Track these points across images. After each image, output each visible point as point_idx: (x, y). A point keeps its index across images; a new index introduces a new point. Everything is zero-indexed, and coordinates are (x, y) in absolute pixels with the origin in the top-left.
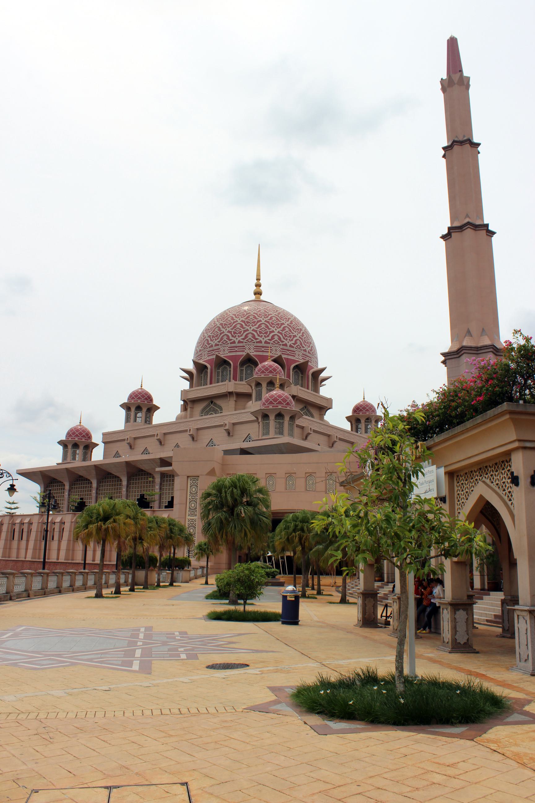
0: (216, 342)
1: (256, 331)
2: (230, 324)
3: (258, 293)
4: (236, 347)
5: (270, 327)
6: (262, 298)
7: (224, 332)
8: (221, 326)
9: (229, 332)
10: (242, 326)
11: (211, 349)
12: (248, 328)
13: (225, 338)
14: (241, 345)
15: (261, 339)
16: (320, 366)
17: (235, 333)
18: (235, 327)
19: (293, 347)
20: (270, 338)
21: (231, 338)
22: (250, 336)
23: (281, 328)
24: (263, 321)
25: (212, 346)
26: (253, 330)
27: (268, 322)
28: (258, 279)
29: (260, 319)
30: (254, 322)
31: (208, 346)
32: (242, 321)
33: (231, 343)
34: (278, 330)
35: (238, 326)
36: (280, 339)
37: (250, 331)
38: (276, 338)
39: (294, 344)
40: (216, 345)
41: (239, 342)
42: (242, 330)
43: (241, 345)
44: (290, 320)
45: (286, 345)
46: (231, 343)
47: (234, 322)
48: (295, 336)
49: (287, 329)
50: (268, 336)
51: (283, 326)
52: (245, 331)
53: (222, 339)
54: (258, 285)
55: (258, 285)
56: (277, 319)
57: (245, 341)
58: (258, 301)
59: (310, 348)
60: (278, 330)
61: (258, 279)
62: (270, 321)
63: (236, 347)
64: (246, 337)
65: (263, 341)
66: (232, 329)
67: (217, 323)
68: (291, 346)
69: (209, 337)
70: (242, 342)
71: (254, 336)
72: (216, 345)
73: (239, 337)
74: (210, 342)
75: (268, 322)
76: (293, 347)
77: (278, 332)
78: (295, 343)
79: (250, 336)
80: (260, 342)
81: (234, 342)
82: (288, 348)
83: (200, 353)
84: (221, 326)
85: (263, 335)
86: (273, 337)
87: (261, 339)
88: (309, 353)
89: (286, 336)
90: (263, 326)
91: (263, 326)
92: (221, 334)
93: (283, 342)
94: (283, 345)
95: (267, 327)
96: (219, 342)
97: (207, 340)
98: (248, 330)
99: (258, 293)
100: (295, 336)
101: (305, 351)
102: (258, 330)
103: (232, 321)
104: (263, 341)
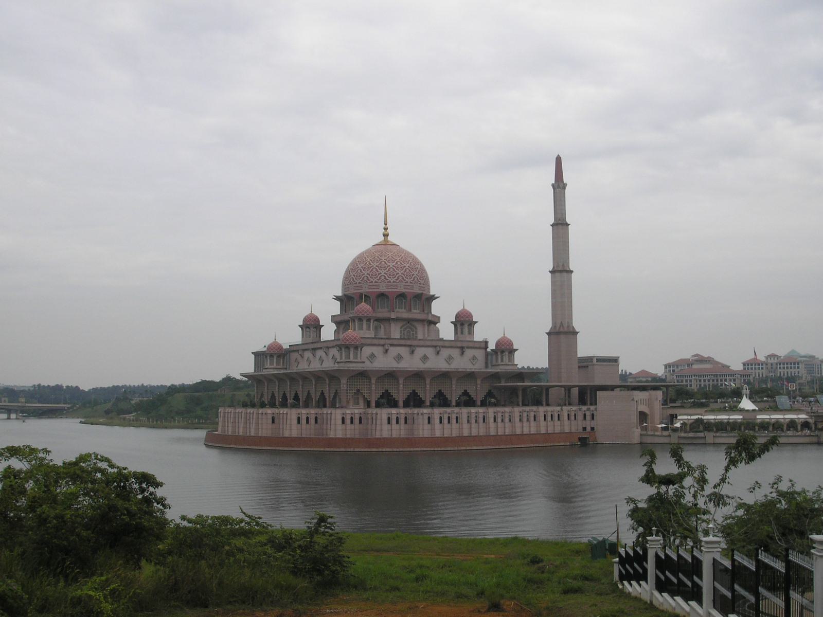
0: (359, 281)
1: (387, 274)
2: (368, 268)
3: (386, 235)
4: (374, 285)
5: (396, 270)
6: (389, 238)
7: (364, 274)
8: (362, 269)
9: (368, 274)
10: (377, 270)
11: (356, 285)
12: (381, 271)
13: (365, 278)
14: (377, 284)
15: (390, 279)
16: (432, 293)
17: (372, 275)
18: (372, 270)
19: (412, 283)
20: (396, 278)
21: (370, 279)
22: (383, 278)
23: (404, 271)
24: (391, 266)
25: (356, 283)
26: (385, 273)
27: (395, 267)
28: (386, 224)
29: (389, 264)
30: (385, 267)
31: (354, 283)
32: (377, 266)
33: (370, 283)
34: (401, 272)
35: (374, 270)
36: (403, 278)
37: (383, 274)
38: (401, 278)
39: (413, 281)
40: (359, 283)
41: (376, 282)
42: (377, 273)
43: (377, 284)
44: (410, 262)
45: (407, 282)
46: (370, 283)
47: (372, 267)
48: (413, 275)
49: (408, 271)
50: (395, 277)
51: (405, 268)
52: (379, 274)
53: (363, 279)
54: (386, 229)
55: (386, 229)
56: (401, 263)
57: (379, 281)
58: (386, 243)
59: (424, 281)
60: (401, 272)
61: (386, 224)
62: (396, 266)
63: (374, 285)
64: (380, 278)
65: (392, 281)
66: (370, 272)
67: (359, 265)
68: (411, 283)
69: (354, 275)
70: (377, 282)
71: (385, 278)
72: (359, 283)
73: (375, 278)
74: (355, 279)
75: (395, 267)
76: (412, 283)
77: (402, 273)
78: (414, 279)
79: (383, 278)
80: (390, 282)
81: (372, 282)
82: (409, 284)
83: (347, 286)
84: (362, 269)
85: (391, 277)
86: (398, 278)
87: (390, 279)
88: (423, 284)
89: (407, 276)
90: (392, 270)
91: (392, 270)
92: (362, 275)
93: (405, 280)
94: (406, 282)
95: (394, 270)
96: (361, 281)
97: (353, 278)
98: (381, 273)
99: (386, 235)
100: (413, 275)
101: (420, 284)
102: (388, 273)
103: (370, 266)
104: (392, 281)
